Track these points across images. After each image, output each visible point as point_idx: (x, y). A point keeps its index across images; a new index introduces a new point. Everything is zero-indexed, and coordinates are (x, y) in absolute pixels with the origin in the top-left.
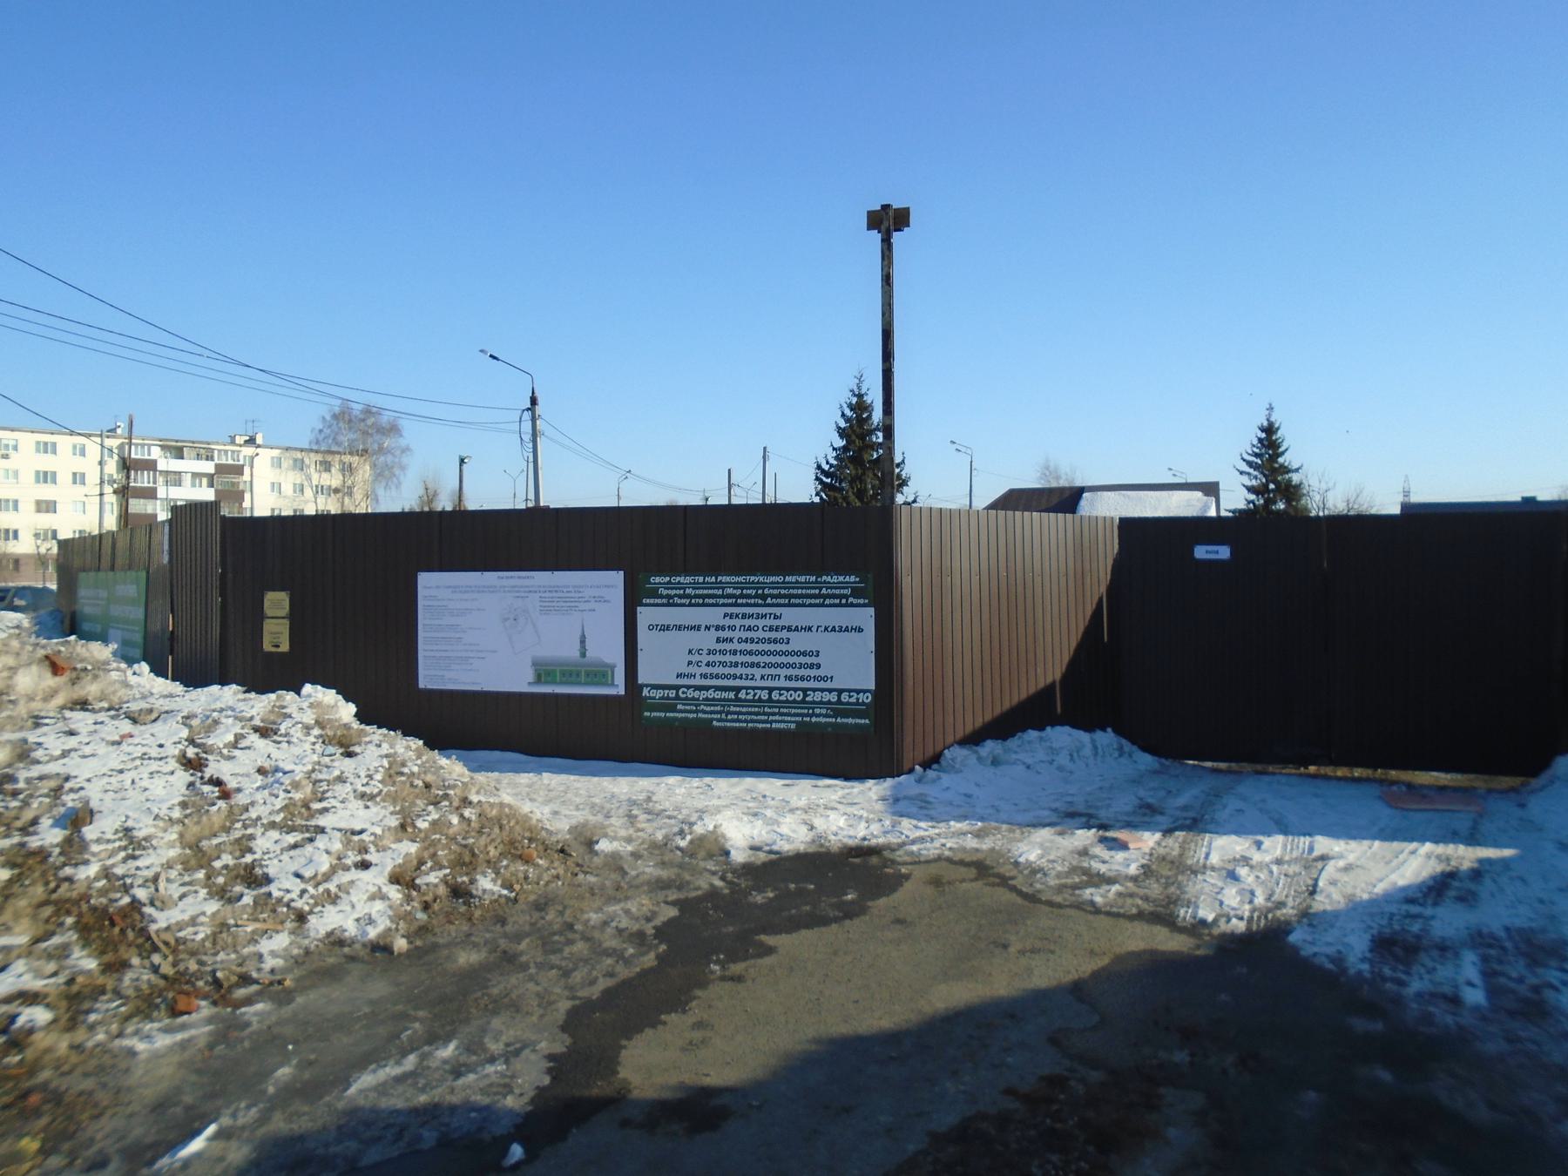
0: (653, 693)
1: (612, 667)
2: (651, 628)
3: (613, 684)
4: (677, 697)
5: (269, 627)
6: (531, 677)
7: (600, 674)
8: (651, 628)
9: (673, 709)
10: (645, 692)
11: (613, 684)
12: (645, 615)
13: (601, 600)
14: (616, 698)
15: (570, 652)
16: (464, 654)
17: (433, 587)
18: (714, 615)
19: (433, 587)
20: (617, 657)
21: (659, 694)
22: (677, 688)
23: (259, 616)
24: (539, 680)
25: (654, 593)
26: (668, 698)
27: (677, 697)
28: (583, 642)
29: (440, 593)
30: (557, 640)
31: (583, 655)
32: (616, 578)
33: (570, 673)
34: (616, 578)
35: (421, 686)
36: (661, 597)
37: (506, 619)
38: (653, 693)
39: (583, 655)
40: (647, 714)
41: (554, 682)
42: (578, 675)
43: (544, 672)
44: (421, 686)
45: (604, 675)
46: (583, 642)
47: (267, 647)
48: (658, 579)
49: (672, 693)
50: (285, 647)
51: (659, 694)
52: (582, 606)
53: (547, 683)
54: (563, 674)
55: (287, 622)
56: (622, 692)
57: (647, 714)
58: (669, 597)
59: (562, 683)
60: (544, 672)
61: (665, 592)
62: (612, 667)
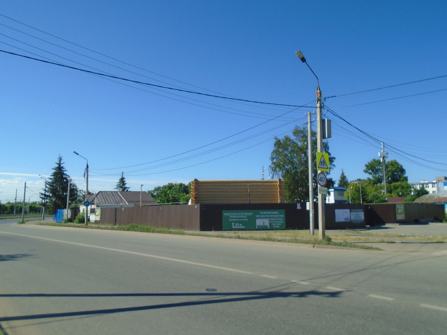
7: (349, 219)
18: (355, 213)
20: (349, 217)
34: (348, 210)
43: (345, 219)
60: (345, 219)
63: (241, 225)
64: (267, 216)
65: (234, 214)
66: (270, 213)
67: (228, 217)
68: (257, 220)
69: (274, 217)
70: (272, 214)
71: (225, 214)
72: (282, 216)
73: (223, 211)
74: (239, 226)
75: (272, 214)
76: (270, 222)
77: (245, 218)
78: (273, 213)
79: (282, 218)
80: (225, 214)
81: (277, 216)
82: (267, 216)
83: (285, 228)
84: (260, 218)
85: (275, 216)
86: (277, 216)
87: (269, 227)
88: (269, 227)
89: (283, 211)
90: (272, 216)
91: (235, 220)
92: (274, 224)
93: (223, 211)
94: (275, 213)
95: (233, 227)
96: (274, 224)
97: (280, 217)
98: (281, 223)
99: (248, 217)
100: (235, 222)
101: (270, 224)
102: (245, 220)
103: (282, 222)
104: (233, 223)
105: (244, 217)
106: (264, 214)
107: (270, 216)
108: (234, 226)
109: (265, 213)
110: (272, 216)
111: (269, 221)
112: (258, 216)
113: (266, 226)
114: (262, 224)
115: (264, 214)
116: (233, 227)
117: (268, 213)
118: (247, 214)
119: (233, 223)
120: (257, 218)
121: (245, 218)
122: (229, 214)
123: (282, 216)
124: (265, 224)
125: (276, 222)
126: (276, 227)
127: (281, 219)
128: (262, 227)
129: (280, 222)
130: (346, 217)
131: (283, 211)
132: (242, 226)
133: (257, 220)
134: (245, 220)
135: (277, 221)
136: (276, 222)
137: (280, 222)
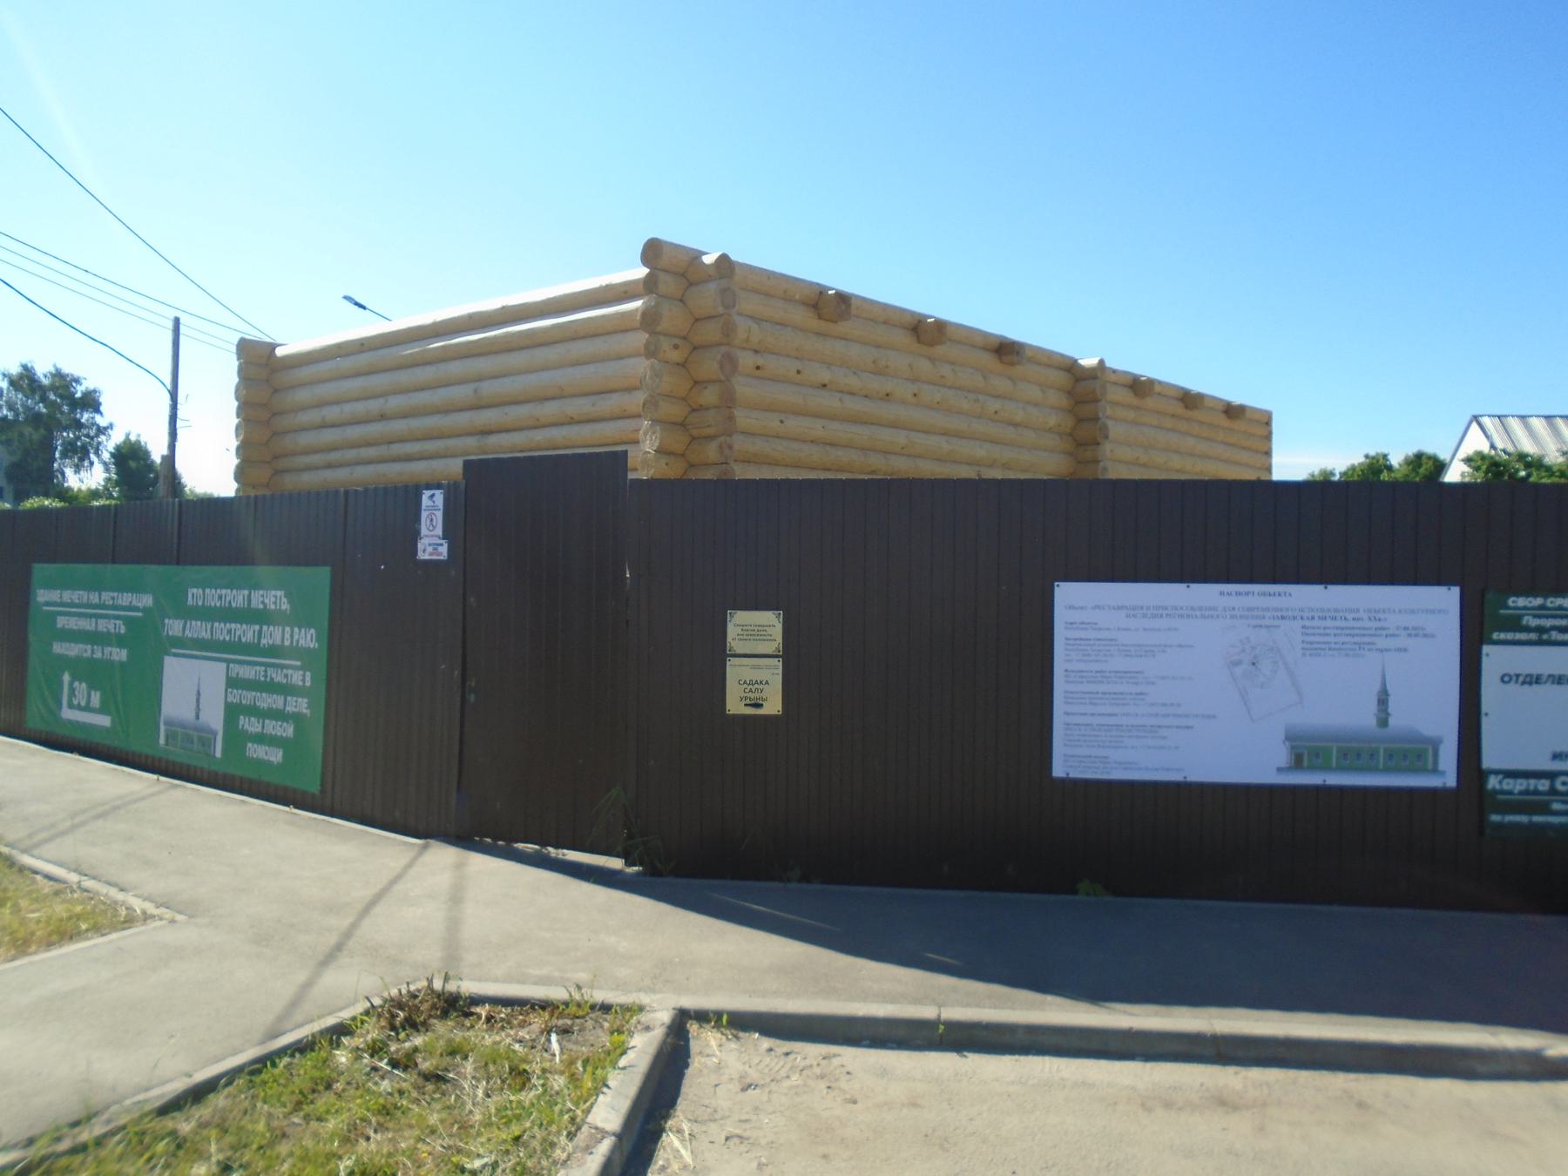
0: (1508, 784)
1: (1435, 744)
2: (1505, 679)
3: (1435, 770)
4: (1553, 791)
5: (737, 674)
6: (1282, 756)
7: (1417, 753)
8: (1505, 679)
9: (1544, 809)
10: (1493, 782)
11: (1435, 770)
12: (1495, 659)
13: (1415, 632)
14: (1433, 792)
17: (1083, 609)
19: (1083, 609)
20: (1443, 724)
21: (1519, 785)
22: (1551, 776)
24: (1298, 763)
25: (1514, 624)
26: (1536, 792)
27: (1553, 791)
28: (1383, 700)
29: (1091, 617)
30: (1336, 700)
31: (1383, 722)
32: (1445, 601)
34: (1445, 601)
35: (1058, 771)
36: (1528, 629)
37: (1239, 663)
38: (1508, 784)
39: (1383, 722)
40: (1495, 818)
41: (1327, 768)
42: (1372, 756)
44: (1058, 771)
45: (1420, 756)
46: (1383, 700)
48: (1522, 602)
49: (1543, 785)
50: (773, 705)
51: (1519, 785)
52: (1381, 643)
53: (1313, 768)
55: (778, 664)
56: (1450, 780)
57: (1495, 818)
58: (1540, 630)
59: (1341, 769)
60: (1305, 750)
61: (1534, 622)
62: (1435, 744)
66: (237, 598)
68: (170, 664)
73: (40, 570)
74: (87, 708)
76: (236, 696)
82: (222, 631)
83: (313, 786)
87: (218, 754)
90: (247, 633)
93: (40, 570)
98: (297, 718)
104: (66, 678)
111: (233, 683)
116: (68, 714)
118: (126, 599)
125: (267, 701)
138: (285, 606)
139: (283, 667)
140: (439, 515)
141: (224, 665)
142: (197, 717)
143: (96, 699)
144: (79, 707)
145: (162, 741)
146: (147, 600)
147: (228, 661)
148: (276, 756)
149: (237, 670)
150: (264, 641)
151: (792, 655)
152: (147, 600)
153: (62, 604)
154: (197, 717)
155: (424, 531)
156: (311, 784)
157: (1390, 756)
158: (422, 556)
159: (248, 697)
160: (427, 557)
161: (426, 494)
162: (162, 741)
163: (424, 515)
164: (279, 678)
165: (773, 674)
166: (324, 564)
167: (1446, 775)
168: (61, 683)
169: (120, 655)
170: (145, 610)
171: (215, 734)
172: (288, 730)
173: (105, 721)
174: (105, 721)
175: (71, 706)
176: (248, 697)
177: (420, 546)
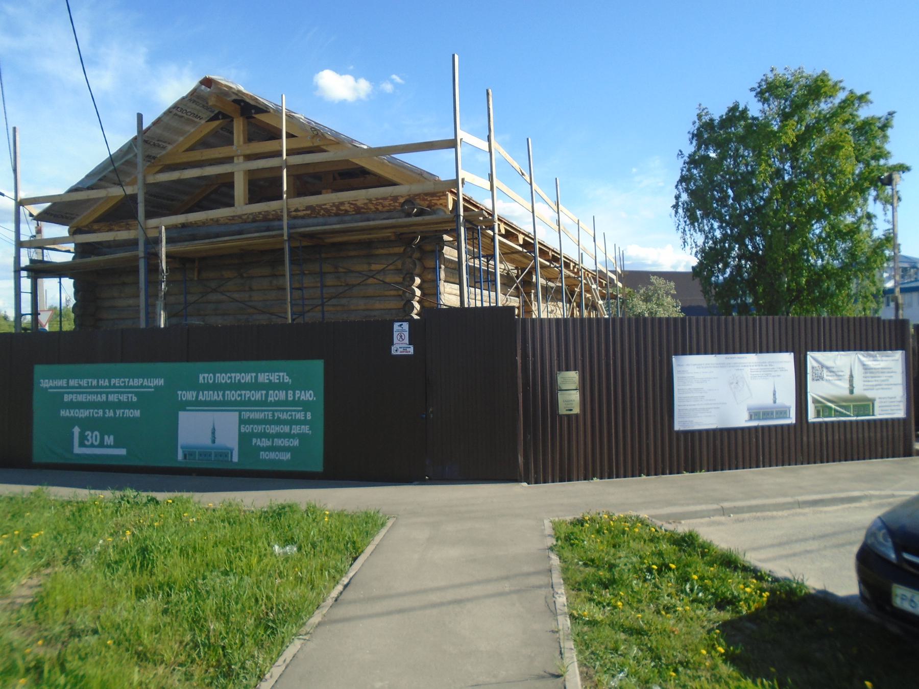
1: (789, 408)
5: (561, 397)
6: (746, 416)
14: (789, 426)
15: (767, 401)
16: (705, 407)
23: (554, 390)
24: (751, 419)
31: (775, 402)
33: (766, 413)
37: (732, 383)
39: (775, 402)
41: (759, 419)
42: (772, 413)
44: (677, 427)
45: (785, 412)
47: (562, 411)
52: (773, 374)
53: (755, 419)
54: (764, 414)
59: (764, 419)
60: (754, 414)
63: (109, 440)
64: (232, 395)
65: (84, 382)
66: (248, 378)
67: (57, 400)
68: (182, 415)
69: (264, 403)
70: (255, 386)
71: (45, 383)
72: (308, 396)
73: (39, 369)
74: (102, 445)
75: (255, 386)
76: (247, 429)
77: (129, 405)
78: (263, 378)
79: (306, 406)
80: (45, 383)
81: (282, 395)
82: (232, 395)
84: (198, 405)
85: (274, 396)
86: (282, 395)
87: (235, 459)
88: (235, 459)
89: (317, 367)
90: (258, 395)
91: (84, 414)
92: (265, 443)
93: (39, 369)
94: (274, 377)
95: (77, 450)
96: (265, 443)
97: (296, 403)
98: (301, 436)
99: (144, 399)
100: (88, 424)
101: (244, 439)
102: (129, 413)
103: (306, 429)
104: (76, 430)
105: (124, 398)
106: (215, 387)
107: (247, 394)
108: (82, 444)
109: (222, 378)
110: (258, 395)
111: (242, 422)
112: (190, 395)
113: (225, 453)
114: (206, 441)
115: (215, 387)
116: (77, 450)
117: (237, 377)
118: (137, 382)
119: (76, 430)
120: (184, 406)
121: (129, 405)
122: (63, 383)
123: (308, 396)
124: (221, 441)
125: (273, 429)
126: (272, 455)
127: (300, 416)
128: (205, 453)
129: (296, 430)
130: (765, 400)
131: (317, 367)
132: (116, 445)
133: (182, 415)
134: (129, 413)
135: (279, 422)
136: (273, 429)
137: (296, 430)
138: (287, 379)
139: (287, 411)
140: (407, 334)
141: (237, 413)
142: (214, 442)
143: (109, 440)
144: (92, 446)
145: (180, 456)
146: (161, 382)
147: (240, 411)
148: (287, 456)
149: (246, 415)
150: (269, 399)
151: (582, 389)
152: (161, 382)
153: (68, 387)
154: (214, 442)
155: (395, 341)
156: (317, 465)
157: (777, 413)
158: (394, 352)
159: (258, 429)
160: (398, 353)
161: (396, 326)
162: (180, 456)
163: (395, 334)
164: (285, 416)
165: (575, 396)
166: (318, 358)
167: (792, 420)
168: (73, 433)
169: (137, 413)
170: (156, 387)
171: (232, 451)
172: (296, 443)
173: (123, 452)
174: (123, 452)
175: (82, 444)
176: (258, 429)
177: (393, 348)
